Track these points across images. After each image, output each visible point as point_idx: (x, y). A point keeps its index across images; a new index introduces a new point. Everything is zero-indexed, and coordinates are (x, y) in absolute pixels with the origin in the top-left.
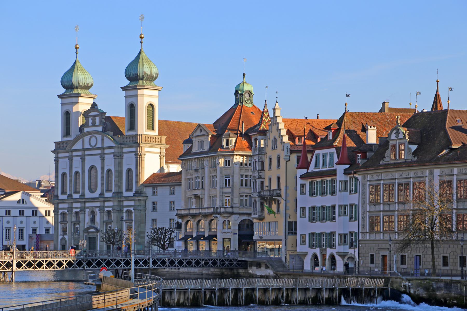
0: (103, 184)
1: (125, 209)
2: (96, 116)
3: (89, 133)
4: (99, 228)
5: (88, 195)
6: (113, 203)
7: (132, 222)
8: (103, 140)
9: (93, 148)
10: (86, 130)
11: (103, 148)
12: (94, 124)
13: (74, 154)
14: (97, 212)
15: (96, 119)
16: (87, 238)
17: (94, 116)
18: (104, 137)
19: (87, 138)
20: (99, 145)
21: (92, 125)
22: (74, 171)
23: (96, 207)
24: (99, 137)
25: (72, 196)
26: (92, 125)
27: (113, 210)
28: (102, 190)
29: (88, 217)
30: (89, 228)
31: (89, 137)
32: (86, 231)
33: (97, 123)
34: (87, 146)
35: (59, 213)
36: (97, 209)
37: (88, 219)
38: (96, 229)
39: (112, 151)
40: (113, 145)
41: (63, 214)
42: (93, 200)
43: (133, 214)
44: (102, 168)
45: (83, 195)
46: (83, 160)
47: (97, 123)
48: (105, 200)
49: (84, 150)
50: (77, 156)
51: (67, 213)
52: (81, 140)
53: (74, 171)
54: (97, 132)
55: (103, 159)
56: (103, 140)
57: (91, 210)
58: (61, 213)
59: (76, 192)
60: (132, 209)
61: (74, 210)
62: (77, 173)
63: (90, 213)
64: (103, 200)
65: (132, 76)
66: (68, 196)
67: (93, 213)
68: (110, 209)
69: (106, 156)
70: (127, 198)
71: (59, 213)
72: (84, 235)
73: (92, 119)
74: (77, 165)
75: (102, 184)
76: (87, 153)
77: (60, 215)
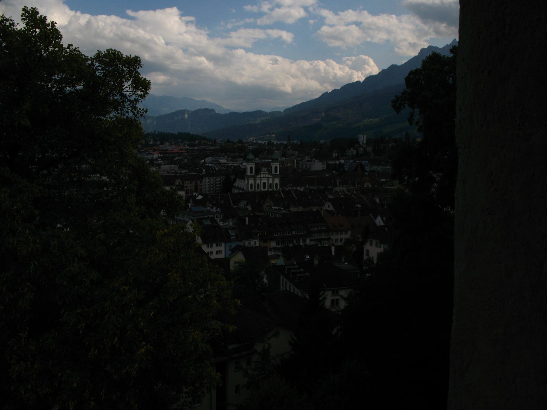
3: (262, 173)
5: (262, 190)
8: (268, 176)
9: (264, 177)
10: (262, 172)
11: (268, 178)
12: (264, 171)
19: (262, 175)
20: (267, 176)
22: (257, 183)
24: (267, 175)
28: (268, 189)
34: (262, 177)
40: (271, 177)
44: (268, 183)
49: (261, 178)
53: (257, 183)
54: (266, 173)
56: (268, 176)
59: (258, 188)
62: (258, 184)
66: (254, 190)
69: (269, 180)
74: (258, 182)
75: (268, 187)
76: (262, 179)
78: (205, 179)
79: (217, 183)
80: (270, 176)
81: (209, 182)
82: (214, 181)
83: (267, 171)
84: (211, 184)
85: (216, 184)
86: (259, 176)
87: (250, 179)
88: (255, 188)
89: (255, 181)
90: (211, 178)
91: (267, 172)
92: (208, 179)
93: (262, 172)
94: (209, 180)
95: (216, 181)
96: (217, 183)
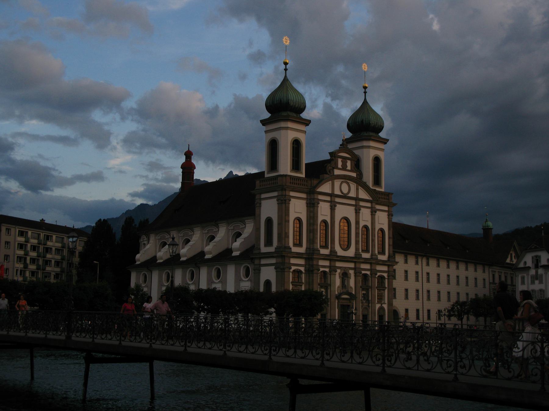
0: (359, 241)
1: (379, 274)
2: (348, 159)
3: (339, 177)
4: (354, 293)
5: (340, 252)
6: (371, 266)
7: (384, 290)
8: (357, 189)
9: (345, 196)
10: (337, 172)
11: (357, 199)
12: (344, 168)
13: (321, 197)
14: (350, 274)
15: (347, 162)
16: (340, 306)
17: (344, 159)
18: (360, 187)
20: (352, 194)
21: (341, 168)
24: (353, 186)
25: (319, 250)
26: (341, 168)
27: (371, 274)
28: (357, 249)
29: (339, 279)
30: (340, 294)
31: (341, 182)
32: (338, 297)
33: (349, 168)
34: (337, 192)
35: (291, 270)
36: (352, 272)
37: (338, 282)
38: (350, 294)
39: (369, 205)
41: (298, 273)
43: (386, 280)
44: (357, 223)
45: (333, 252)
46: (333, 209)
47: (349, 168)
48: (365, 261)
49: (332, 195)
51: (304, 272)
52: (330, 182)
53: (320, 218)
55: (357, 212)
57: (343, 271)
58: (294, 271)
59: (326, 247)
60: (385, 275)
61: (321, 269)
63: (341, 274)
64: (364, 261)
65: (377, 126)
67: (345, 276)
68: (368, 273)
70: (383, 263)
71: (291, 270)
72: (335, 302)
73: (342, 161)
75: (357, 242)
77: (291, 274)
78: (8, 230)
79: (49, 256)
80: (363, 195)
81: (21, 246)
82: (41, 247)
83: (351, 171)
84: (28, 258)
85: (47, 262)
86: (325, 188)
87: (292, 194)
88: (311, 241)
89: (312, 206)
90: (30, 233)
91: (354, 175)
92: (21, 234)
93: (337, 172)
94: (22, 239)
95: (48, 250)
96: (49, 256)
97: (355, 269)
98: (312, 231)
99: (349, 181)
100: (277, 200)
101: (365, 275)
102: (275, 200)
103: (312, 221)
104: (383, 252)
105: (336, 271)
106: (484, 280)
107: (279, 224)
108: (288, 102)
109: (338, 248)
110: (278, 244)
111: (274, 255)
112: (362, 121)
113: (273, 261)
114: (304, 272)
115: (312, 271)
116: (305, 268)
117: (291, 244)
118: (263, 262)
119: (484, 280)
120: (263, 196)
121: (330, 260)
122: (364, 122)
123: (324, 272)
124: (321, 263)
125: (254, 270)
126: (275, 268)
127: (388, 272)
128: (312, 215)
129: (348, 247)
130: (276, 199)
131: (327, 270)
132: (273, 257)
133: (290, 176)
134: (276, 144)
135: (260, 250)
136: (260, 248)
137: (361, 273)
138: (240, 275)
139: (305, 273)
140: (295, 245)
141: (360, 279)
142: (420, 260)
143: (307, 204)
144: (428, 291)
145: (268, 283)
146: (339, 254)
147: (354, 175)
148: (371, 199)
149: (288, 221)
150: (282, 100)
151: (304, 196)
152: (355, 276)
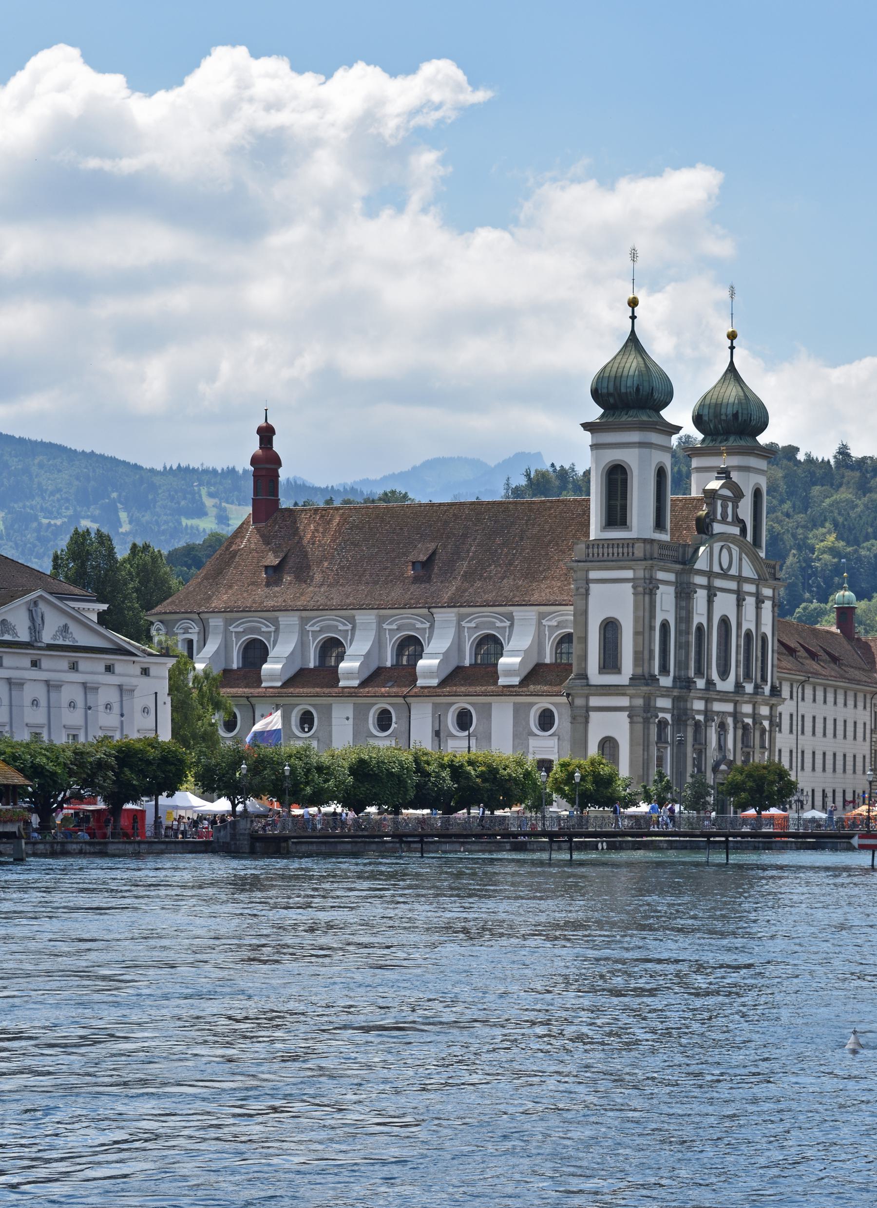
8: (740, 559)
9: (724, 575)
17: (725, 499)
18: (744, 555)
23: (729, 714)
25: (695, 682)
27: (754, 723)
28: (737, 675)
33: (730, 519)
36: (730, 721)
41: (662, 724)
42: (724, 697)
45: (710, 683)
47: (730, 519)
49: (710, 574)
50: (702, 587)
51: (670, 722)
56: (740, 559)
60: (766, 724)
62: (700, 628)
67: (722, 726)
75: (737, 661)
80: (748, 571)
83: (732, 524)
87: (661, 575)
88: (682, 664)
89: (684, 594)
97: (735, 715)
98: (682, 646)
99: (731, 545)
100: (634, 587)
101: (745, 727)
102: (629, 586)
103: (683, 626)
104: (764, 679)
105: (713, 720)
106: (865, 724)
107: (636, 633)
108: (652, 393)
109: (715, 676)
110: (634, 670)
111: (628, 692)
112: (735, 415)
113: (624, 702)
114: (670, 722)
115: (686, 721)
116: (673, 715)
117: (657, 672)
118: (594, 701)
119: (865, 724)
120: (593, 575)
121: (708, 701)
122: (740, 415)
123: (697, 724)
124: (699, 705)
125: (574, 718)
126: (629, 716)
127: (771, 718)
128: (683, 613)
129: (724, 674)
130: (631, 584)
131: (700, 718)
132: (624, 694)
133: (652, 541)
134: (626, 474)
135: (587, 679)
136: (587, 676)
137: (743, 722)
138: (528, 723)
139: (673, 725)
140: (660, 671)
141: (740, 732)
142: (795, 690)
143: (676, 593)
144: (803, 752)
145: (608, 745)
146: (719, 688)
147: (736, 531)
148: (756, 577)
149: (652, 628)
150: (641, 388)
151: (671, 577)
152: (735, 728)
